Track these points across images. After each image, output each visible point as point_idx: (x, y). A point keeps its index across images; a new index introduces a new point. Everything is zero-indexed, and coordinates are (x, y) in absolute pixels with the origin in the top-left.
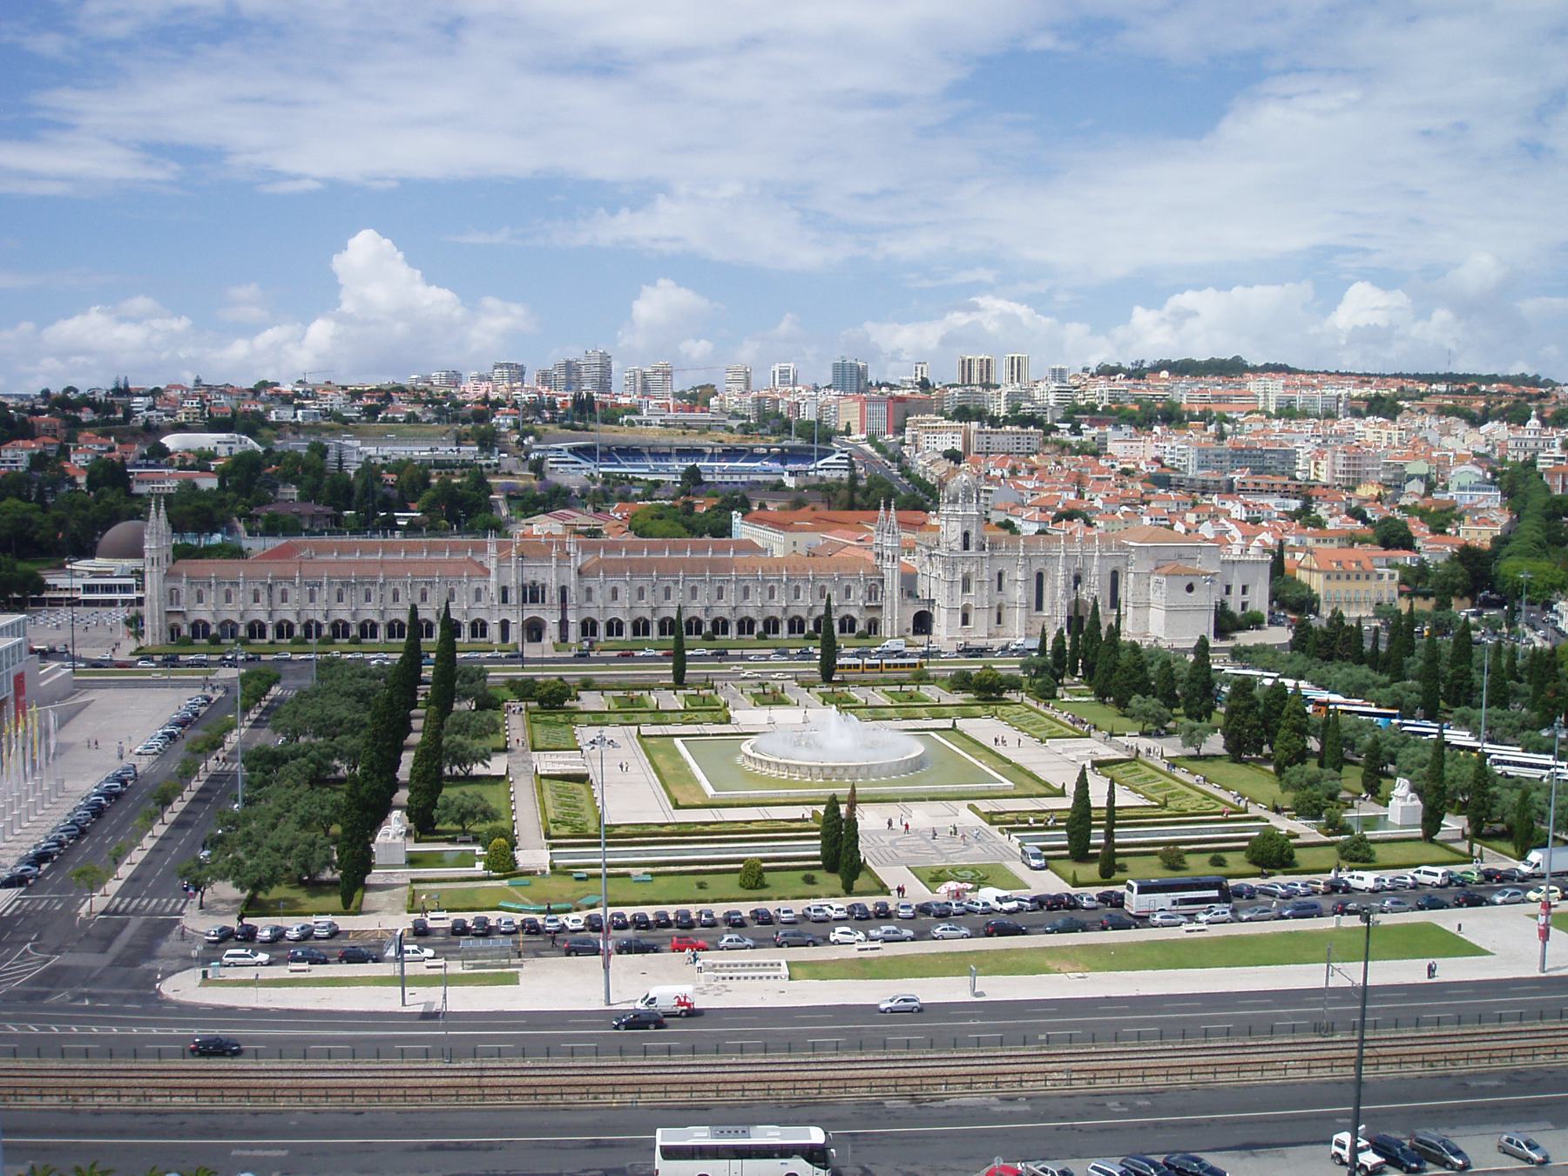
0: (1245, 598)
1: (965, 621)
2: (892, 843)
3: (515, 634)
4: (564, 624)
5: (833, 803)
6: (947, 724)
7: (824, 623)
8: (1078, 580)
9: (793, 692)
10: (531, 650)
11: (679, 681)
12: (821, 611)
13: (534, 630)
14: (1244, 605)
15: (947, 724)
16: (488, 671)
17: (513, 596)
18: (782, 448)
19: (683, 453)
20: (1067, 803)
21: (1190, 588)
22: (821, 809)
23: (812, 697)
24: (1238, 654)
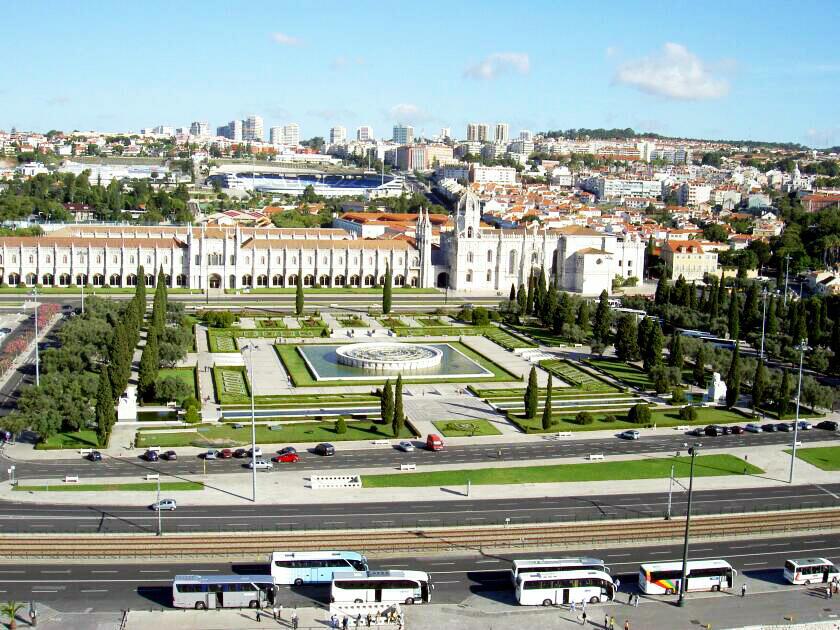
0: (629, 268)
1: (469, 278)
2: (424, 408)
3: (205, 285)
4: (233, 279)
5: (387, 384)
6: (456, 339)
7: (386, 281)
8: (535, 256)
9: (365, 319)
10: (214, 293)
11: (299, 312)
12: (382, 272)
13: (216, 281)
14: (629, 272)
15: (456, 339)
16: (185, 305)
17: (204, 260)
18: (363, 175)
19: (304, 178)
20: (525, 385)
21: (599, 262)
22: (382, 388)
23: (374, 323)
24: (626, 302)
